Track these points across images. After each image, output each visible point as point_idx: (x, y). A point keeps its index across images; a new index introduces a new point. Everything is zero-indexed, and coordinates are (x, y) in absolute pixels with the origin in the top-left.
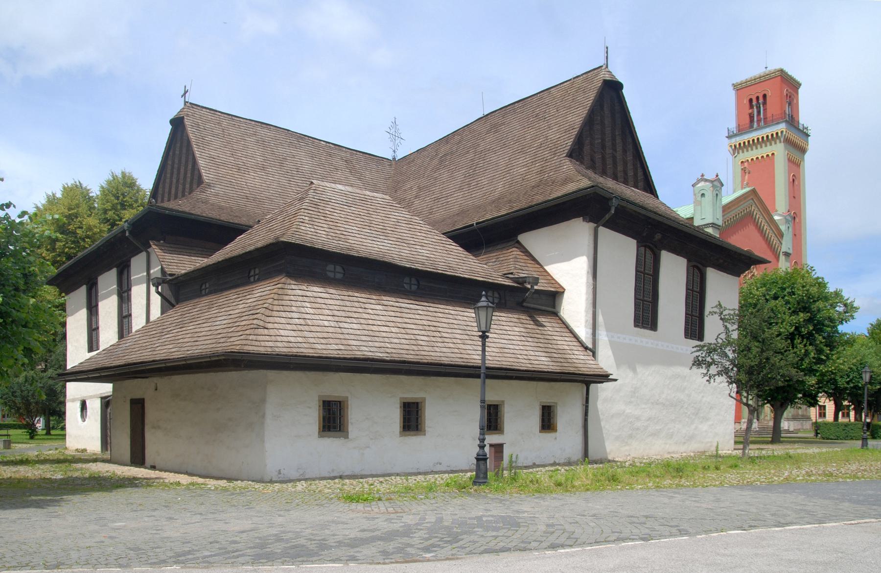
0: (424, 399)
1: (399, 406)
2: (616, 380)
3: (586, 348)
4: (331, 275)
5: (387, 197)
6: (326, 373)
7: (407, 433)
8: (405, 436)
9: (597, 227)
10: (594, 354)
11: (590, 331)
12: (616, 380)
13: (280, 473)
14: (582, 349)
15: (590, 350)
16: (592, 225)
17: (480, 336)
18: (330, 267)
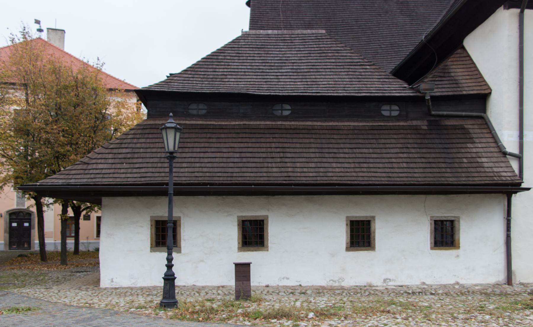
0: (267, 217)
1: (236, 224)
2: (528, 189)
3: (505, 154)
4: (195, 112)
5: (324, 32)
6: (158, 197)
7: (245, 248)
8: (244, 251)
9: (522, 12)
10: (520, 158)
11: (516, 133)
12: (528, 189)
13: (112, 281)
14: (500, 155)
15: (511, 155)
16: (517, 11)
17: (167, 158)
18: (193, 106)
